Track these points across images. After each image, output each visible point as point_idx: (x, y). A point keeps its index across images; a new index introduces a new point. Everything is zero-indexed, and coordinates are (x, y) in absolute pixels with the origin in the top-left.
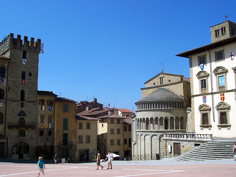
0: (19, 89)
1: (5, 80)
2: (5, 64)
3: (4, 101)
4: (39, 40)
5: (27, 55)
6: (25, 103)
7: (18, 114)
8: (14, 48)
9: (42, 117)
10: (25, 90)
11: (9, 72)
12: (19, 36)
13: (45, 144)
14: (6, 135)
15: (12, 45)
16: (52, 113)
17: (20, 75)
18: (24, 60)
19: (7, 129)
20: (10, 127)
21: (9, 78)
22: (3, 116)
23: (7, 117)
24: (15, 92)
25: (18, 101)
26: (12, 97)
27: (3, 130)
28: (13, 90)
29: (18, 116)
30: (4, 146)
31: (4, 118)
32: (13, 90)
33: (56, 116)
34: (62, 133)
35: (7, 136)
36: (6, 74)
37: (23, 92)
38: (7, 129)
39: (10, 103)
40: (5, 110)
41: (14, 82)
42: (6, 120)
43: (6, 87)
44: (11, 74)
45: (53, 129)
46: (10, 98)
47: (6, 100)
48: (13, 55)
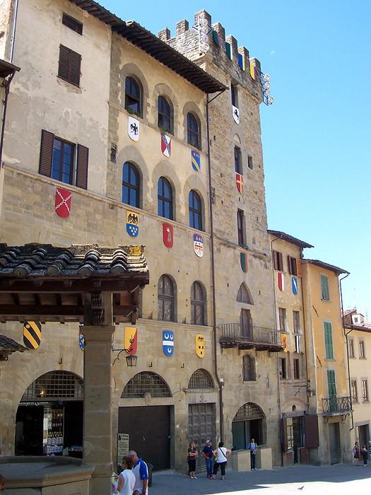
1: (203, 160)
2: (199, 103)
3: (205, 236)
4: (258, 63)
5: (240, 94)
6: (249, 257)
7: (236, 293)
9: (283, 310)
10: (245, 209)
13: (294, 407)
14: (219, 373)
16: (299, 301)
17: (231, 155)
19: (218, 353)
20: (227, 343)
24: (225, 211)
27: (210, 351)
33: (310, 311)
34: (326, 370)
36: (204, 142)
37: (240, 213)
39: (219, 250)
40: (209, 271)
44: (213, 144)
45: (304, 354)
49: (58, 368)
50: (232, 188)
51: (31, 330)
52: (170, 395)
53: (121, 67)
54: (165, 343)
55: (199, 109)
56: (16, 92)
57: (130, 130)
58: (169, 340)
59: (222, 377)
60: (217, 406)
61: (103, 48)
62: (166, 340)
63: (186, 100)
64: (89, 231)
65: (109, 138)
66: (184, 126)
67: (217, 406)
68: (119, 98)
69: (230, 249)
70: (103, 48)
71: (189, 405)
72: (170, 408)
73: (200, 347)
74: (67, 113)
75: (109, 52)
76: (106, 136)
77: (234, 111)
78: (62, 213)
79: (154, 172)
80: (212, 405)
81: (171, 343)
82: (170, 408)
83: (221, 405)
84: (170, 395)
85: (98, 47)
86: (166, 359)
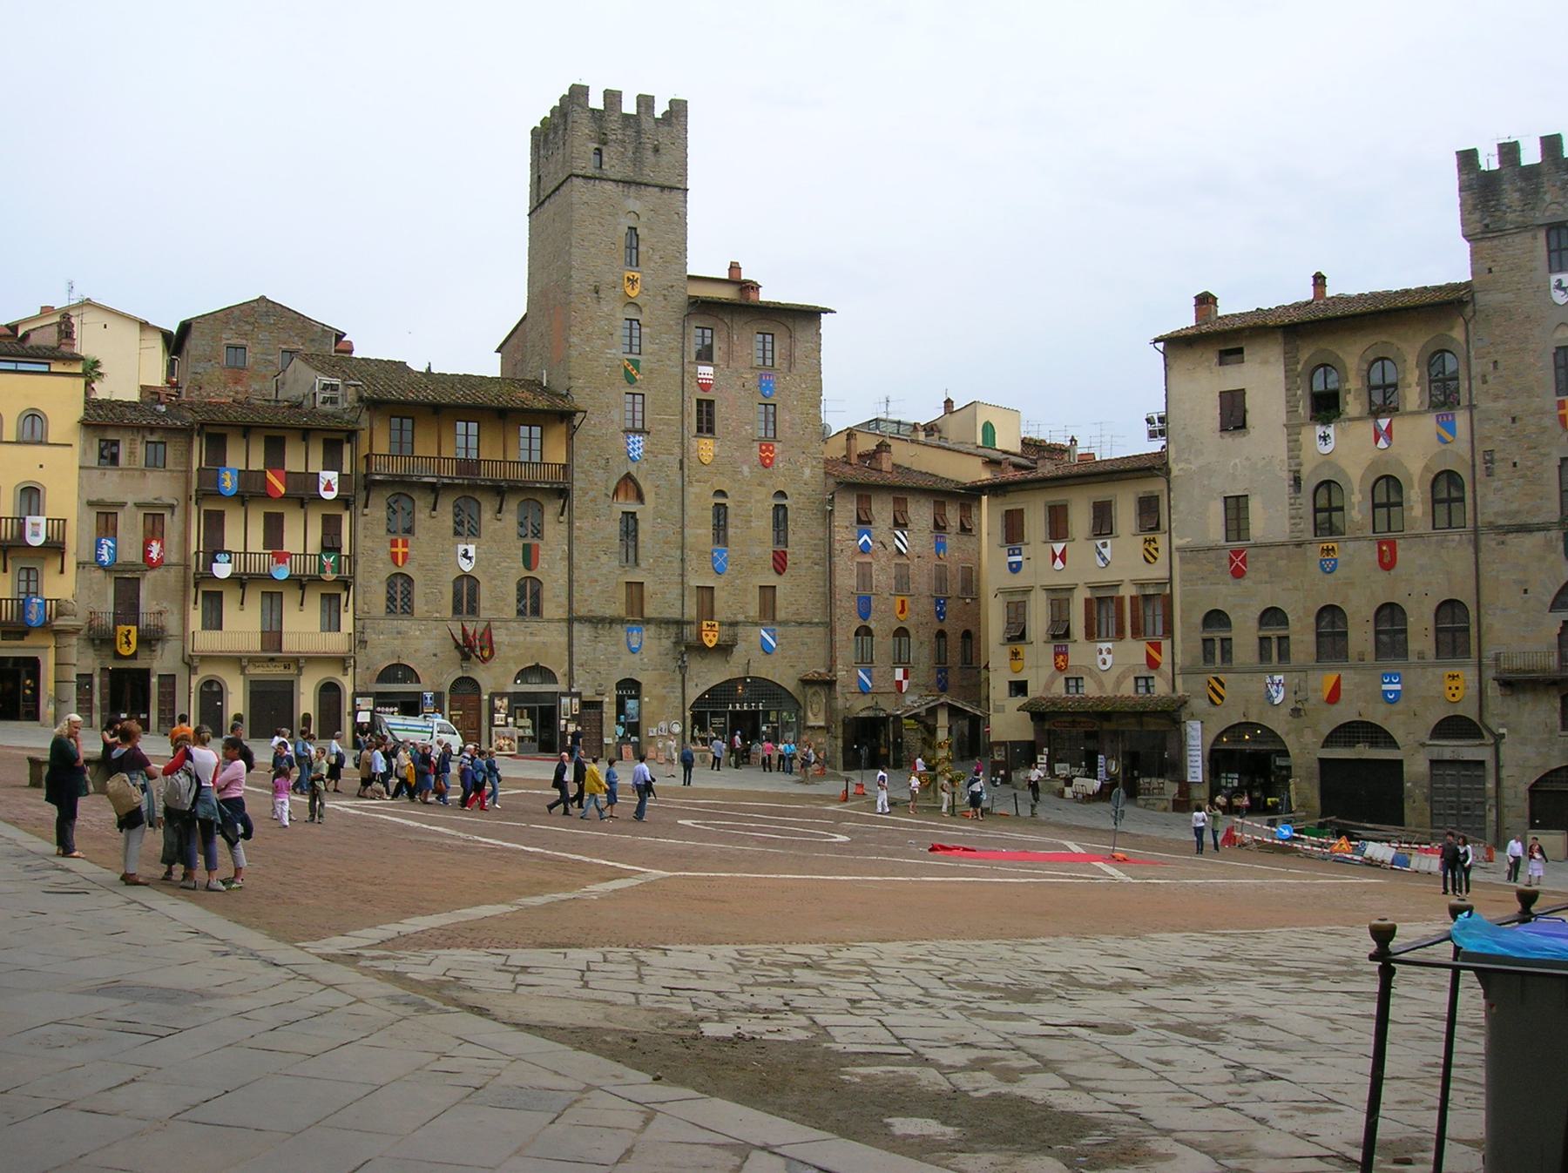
0: (1544, 455)
2: (1451, 328)
7: (1549, 599)
8: (1487, 226)
11: (1476, 369)
12: (1509, 151)
15: (1477, 216)
18: (1560, 281)
21: (1484, 404)
22: (1468, 616)
23: (1485, 621)
25: (1544, 528)
26: (1514, 507)
27: (1474, 692)
28: (1515, 464)
29: (1550, 611)
30: (1482, 779)
31: (1473, 631)
32: (1515, 464)
35: (1492, 722)
36: (1464, 385)
38: (1493, 690)
40: (1473, 583)
41: (1514, 420)
42: (1484, 640)
43: (1468, 457)
44: (1490, 378)
46: (1497, 514)
47: (1476, 530)
48: (1490, 271)
49: (1244, 720)
50: (1544, 430)
51: (1213, 689)
52: (1399, 748)
53: (1299, 367)
54: (1385, 687)
55: (1453, 340)
56: (1181, 473)
57: (1319, 442)
58: (1391, 682)
59: (1503, 726)
60: (1490, 765)
61: (1272, 359)
62: (1384, 683)
63: (1419, 346)
64: (1272, 582)
65: (1290, 466)
66: (1418, 384)
67: (1490, 765)
68: (1301, 410)
69: (1535, 533)
70: (1272, 359)
71: (1432, 762)
72: (1400, 762)
73: (1450, 688)
74: (1236, 464)
75: (1282, 359)
76: (1286, 467)
77: (1553, 282)
78: (1238, 573)
79: (1363, 478)
80: (1481, 763)
81: (1398, 687)
82: (1400, 762)
83: (1498, 767)
84: (1399, 748)
85: (1265, 362)
86: (1389, 706)
